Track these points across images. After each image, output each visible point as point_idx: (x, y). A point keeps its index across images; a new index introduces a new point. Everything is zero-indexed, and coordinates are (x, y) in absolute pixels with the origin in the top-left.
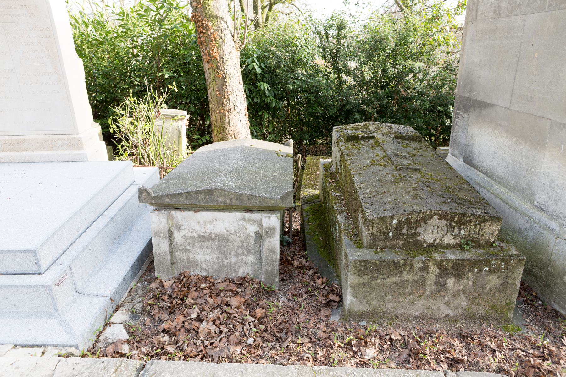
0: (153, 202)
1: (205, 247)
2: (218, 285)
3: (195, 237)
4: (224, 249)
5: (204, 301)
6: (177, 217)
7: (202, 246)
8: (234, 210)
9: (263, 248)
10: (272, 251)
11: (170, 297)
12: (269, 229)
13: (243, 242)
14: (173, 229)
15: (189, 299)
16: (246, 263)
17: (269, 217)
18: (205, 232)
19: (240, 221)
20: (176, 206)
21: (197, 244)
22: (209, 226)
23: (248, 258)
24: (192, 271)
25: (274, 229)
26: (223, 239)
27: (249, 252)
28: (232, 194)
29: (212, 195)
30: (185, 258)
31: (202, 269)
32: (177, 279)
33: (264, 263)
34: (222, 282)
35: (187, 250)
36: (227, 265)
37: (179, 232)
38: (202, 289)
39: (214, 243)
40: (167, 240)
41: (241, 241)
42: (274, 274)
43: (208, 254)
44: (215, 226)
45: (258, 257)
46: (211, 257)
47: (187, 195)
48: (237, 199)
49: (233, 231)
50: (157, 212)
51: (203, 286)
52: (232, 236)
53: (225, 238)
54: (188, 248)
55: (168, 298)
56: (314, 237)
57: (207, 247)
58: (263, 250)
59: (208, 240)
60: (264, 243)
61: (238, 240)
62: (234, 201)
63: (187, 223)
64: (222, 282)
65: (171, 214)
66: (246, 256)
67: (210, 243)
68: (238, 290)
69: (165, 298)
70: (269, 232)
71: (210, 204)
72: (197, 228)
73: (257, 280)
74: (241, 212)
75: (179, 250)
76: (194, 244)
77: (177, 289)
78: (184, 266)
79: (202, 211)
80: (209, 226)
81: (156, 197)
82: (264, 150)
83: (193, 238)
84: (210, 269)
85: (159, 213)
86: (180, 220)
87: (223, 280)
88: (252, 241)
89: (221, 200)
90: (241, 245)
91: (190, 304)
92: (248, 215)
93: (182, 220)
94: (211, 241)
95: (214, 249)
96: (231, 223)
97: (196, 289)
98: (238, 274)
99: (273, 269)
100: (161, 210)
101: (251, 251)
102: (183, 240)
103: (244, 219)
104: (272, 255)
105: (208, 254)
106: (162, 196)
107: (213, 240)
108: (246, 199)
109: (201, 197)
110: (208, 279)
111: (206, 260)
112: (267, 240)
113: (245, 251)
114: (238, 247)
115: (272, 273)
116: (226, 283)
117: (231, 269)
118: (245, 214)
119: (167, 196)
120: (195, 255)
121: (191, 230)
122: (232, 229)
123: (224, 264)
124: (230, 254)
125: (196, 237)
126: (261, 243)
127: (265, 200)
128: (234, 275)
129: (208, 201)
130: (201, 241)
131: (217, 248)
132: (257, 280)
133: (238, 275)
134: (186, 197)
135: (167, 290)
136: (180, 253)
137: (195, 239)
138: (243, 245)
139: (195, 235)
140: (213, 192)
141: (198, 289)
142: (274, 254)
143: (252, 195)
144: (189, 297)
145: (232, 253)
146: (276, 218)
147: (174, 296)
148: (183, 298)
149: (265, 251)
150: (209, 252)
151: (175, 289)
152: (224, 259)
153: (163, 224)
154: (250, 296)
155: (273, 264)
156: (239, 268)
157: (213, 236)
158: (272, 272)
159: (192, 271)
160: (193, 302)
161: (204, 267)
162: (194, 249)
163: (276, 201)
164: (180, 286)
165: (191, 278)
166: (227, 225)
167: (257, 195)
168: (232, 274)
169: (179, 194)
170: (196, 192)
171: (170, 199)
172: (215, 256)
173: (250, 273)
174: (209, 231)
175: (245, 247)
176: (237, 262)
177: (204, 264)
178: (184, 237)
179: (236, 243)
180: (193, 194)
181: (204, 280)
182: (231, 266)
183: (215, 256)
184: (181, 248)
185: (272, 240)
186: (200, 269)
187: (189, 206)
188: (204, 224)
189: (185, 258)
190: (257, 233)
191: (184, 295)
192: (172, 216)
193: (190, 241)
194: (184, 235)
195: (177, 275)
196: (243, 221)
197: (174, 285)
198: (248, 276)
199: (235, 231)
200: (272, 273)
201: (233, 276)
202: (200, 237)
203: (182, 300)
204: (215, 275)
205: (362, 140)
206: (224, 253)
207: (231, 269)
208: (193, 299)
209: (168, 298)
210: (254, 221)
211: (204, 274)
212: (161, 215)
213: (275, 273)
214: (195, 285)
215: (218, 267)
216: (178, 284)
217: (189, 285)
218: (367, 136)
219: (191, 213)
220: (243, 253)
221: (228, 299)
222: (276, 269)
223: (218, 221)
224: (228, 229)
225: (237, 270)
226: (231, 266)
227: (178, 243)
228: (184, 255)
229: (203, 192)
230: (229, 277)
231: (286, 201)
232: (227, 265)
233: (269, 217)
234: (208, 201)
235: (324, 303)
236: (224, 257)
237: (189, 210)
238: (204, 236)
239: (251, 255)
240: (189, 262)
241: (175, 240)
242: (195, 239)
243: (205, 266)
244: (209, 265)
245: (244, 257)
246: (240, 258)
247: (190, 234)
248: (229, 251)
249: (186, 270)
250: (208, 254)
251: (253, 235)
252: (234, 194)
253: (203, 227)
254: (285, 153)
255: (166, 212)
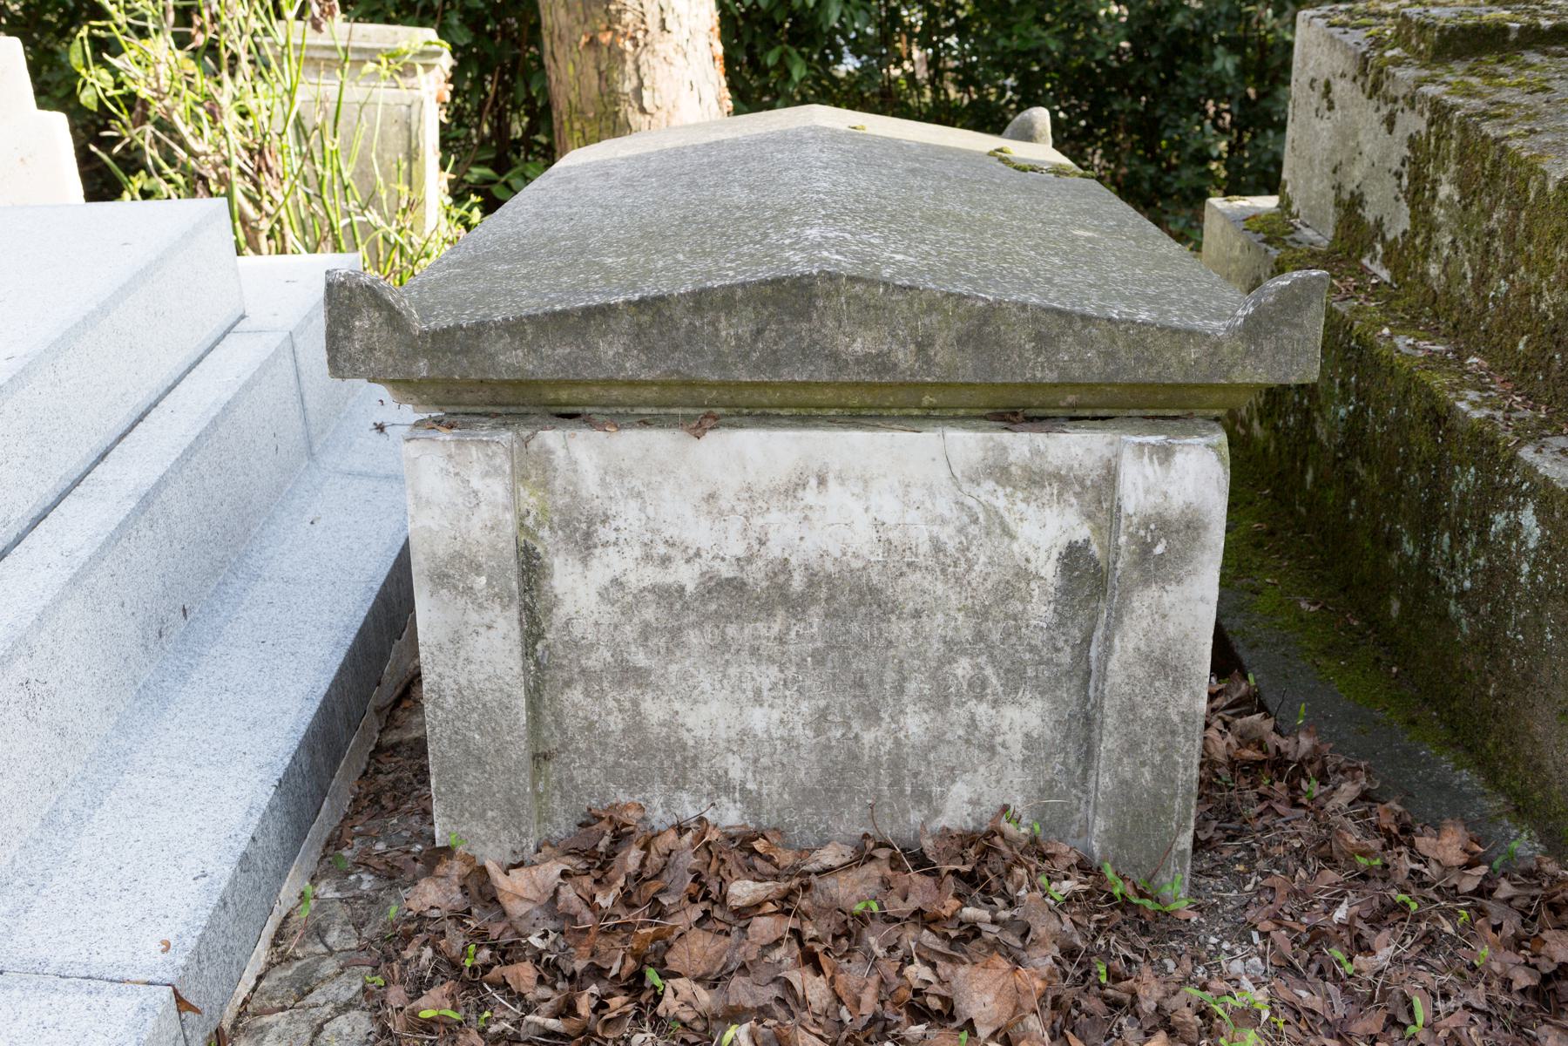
0: (422, 368)
1: (745, 654)
2: (830, 881)
3: (682, 589)
4: (864, 664)
5: (775, 991)
6: (573, 463)
7: (723, 645)
8: (927, 417)
9: (1108, 650)
10: (1164, 666)
11: (549, 971)
12: (1161, 525)
13: (984, 614)
14: (547, 541)
15: (682, 984)
16: (992, 749)
17: (1165, 454)
18: (749, 560)
19: (974, 481)
20: (564, 395)
21: (693, 637)
22: (775, 516)
23: (1010, 713)
24: (657, 802)
25: (1191, 526)
26: (861, 603)
27: (1014, 678)
28: (932, 307)
29: (803, 315)
30: (616, 723)
31: (722, 785)
32: (576, 853)
33: (1108, 744)
34: (846, 867)
35: (628, 675)
36: (876, 763)
37: (584, 561)
38: (746, 913)
39: (799, 627)
40: (514, 612)
41: (970, 612)
42: (1167, 812)
43: (758, 692)
44: (814, 516)
45: (1074, 708)
46: (776, 715)
47: (645, 319)
48: (962, 342)
49: (925, 548)
50: (445, 435)
51: (742, 890)
52: (915, 577)
53: (873, 590)
54: (640, 659)
55: (541, 981)
56: (1260, 599)
57: (754, 651)
58: (1114, 664)
59: (761, 608)
60: (1119, 619)
61: (954, 601)
62: (941, 354)
63: (634, 504)
64: (846, 867)
65: (534, 445)
66: (996, 703)
67: (776, 628)
68: (969, 912)
69: (523, 974)
70: (1159, 549)
71: (786, 375)
72: (700, 533)
73: (1066, 851)
74: (976, 429)
75: (583, 671)
76: (675, 633)
77: (588, 915)
78: (611, 773)
79: (731, 426)
80: (775, 516)
81: (443, 340)
82: (927, 146)
83: (668, 595)
84: (772, 789)
85: (460, 443)
86: (590, 484)
87: (848, 853)
88: (1040, 611)
89: (858, 346)
90: (967, 634)
91: (687, 1016)
92: (1020, 444)
93: (603, 484)
94: (781, 613)
95: (800, 665)
96: (916, 494)
97: (706, 913)
98: (937, 812)
99: (1164, 776)
100: (465, 426)
101: (1030, 672)
102: (608, 615)
103: (1000, 473)
104: (1164, 693)
105: (758, 692)
106: (480, 329)
107: (796, 606)
108: (1021, 337)
109: (732, 330)
110: (759, 846)
111: (744, 736)
112: (1143, 601)
113: (989, 671)
114: (953, 647)
115: (1159, 806)
116: (871, 869)
117: (896, 782)
118: (1007, 437)
119: (513, 328)
120: (677, 706)
121: (662, 549)
122: (921, 536)
123: (854, 757)
124: (900, 690)
125: (690, 588)
126: (1093, 618)
127: (1141, 343)
128: (915, 817)
129: (774, 360)
130: (722, 618)
131: (819, 658)
132: (1066, 851)
133: (942, 822)
134: (638, 334)
135: (524, 926)
136: (587, 693)
137: (686, 607)
138: (980, 636)
139: (686, 576)
140: (811, 299)
141: (717, 913)
142: (1177, 685)
143: (1060, 312)
144: (673, 966)
145: (912, 687)
146: (1211, 457)
147: (580, 965)
148: (639, 976)
149: (1126, 666)
150: (766, 684)
151: (573, 918)
152: (856, 726)
153: (484, 513)
154: (1056, 951)
155: (1167, 751)
156: (951, 774)
157: (798, 583)
158: (1157, 797)
159: (657, 802)
160: (705, 998)
161: (736, 774)
162: (673, 668)
163: (1218, 345)
164: (605, 900)
165: (661, 845)
166: (889, 508)
167: (1090, 310)
168: (904, 812)
169: (588, 313)
170: (701, 300)
171: (533, 348)
172: (805, 707)
173: (1018, 803)
174: (774, 551)
175: (990, 647)
176: (938, 739)
177: (731, 758)
178: (614, 593)
179: (936, 625)
180: (678, 312)
181: (739, 855)
182: (897, 763)
183: (805, 707)
184: (592, 662)
185: (1171, 596)
186: (708, 787)
187: (647, 394)
188: (742, 507)
189: (616, 723)
190: (1073, 557)
191: (641, 958)
192: (544, 460)
193: (649, 614)
194: (616, 582)
195: (562, 826)
196: (989, 485)
197: (568, 894)
198: (1009, 828)
199: (938, 547)
200: (1159, 806)
201: (911, 823)
202: (715, 587)
203: (634, 984)
204: (799, 823)
205: (1527, 47)
206: (860, 684)
207: (896, 782)
208: (698, 980)
209: (541, 981)
210: (1063, 480)
211: (731, 816)
212: (474, 451)
213: (1178, 804)
214: (694, 888)
215: (817, 770)
216: (587, 882)
217: (662, 891)
218: (1554, 29)
219: (661, 441)
220: (978, 687)
221: (918, 972)
222: (1181, 776)
223: (832, 484)
224: (894, 535)
225: (936, 790)
226: (897, 763)
227: (577, 632)
228: (611, 704)
229: (746, 301)
230: (888, 831)
231: (1279, 349)
232: (876, 763)
233: (1165, 454)
234: (774, 360)
235: (1523, 991)
236: (859, 709)
237: (645, 423)
238: (736, 587)
239: (1025, 696)
240: (643, 749)
241: (560, 614)
242: (686, 607)
243: (736, 769)
244: (765, 761)
245: (982, 710)
246: (958, 714)
247: (652, 575)
248: (890, 676)
249: (623, 797)
250: (758, 698)
251: (1049, 570)
252: (949, 305)
253: (736, 523)
254: (1049, 163)
255: (506, 436)
